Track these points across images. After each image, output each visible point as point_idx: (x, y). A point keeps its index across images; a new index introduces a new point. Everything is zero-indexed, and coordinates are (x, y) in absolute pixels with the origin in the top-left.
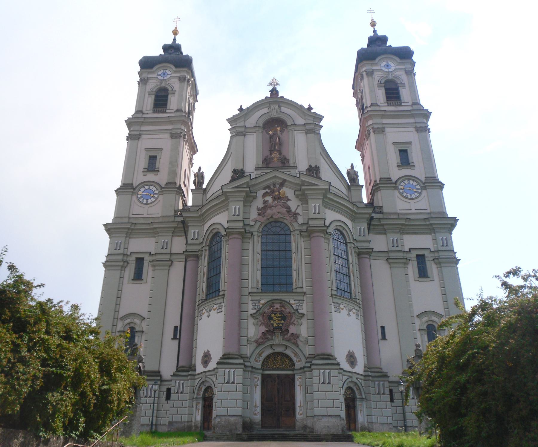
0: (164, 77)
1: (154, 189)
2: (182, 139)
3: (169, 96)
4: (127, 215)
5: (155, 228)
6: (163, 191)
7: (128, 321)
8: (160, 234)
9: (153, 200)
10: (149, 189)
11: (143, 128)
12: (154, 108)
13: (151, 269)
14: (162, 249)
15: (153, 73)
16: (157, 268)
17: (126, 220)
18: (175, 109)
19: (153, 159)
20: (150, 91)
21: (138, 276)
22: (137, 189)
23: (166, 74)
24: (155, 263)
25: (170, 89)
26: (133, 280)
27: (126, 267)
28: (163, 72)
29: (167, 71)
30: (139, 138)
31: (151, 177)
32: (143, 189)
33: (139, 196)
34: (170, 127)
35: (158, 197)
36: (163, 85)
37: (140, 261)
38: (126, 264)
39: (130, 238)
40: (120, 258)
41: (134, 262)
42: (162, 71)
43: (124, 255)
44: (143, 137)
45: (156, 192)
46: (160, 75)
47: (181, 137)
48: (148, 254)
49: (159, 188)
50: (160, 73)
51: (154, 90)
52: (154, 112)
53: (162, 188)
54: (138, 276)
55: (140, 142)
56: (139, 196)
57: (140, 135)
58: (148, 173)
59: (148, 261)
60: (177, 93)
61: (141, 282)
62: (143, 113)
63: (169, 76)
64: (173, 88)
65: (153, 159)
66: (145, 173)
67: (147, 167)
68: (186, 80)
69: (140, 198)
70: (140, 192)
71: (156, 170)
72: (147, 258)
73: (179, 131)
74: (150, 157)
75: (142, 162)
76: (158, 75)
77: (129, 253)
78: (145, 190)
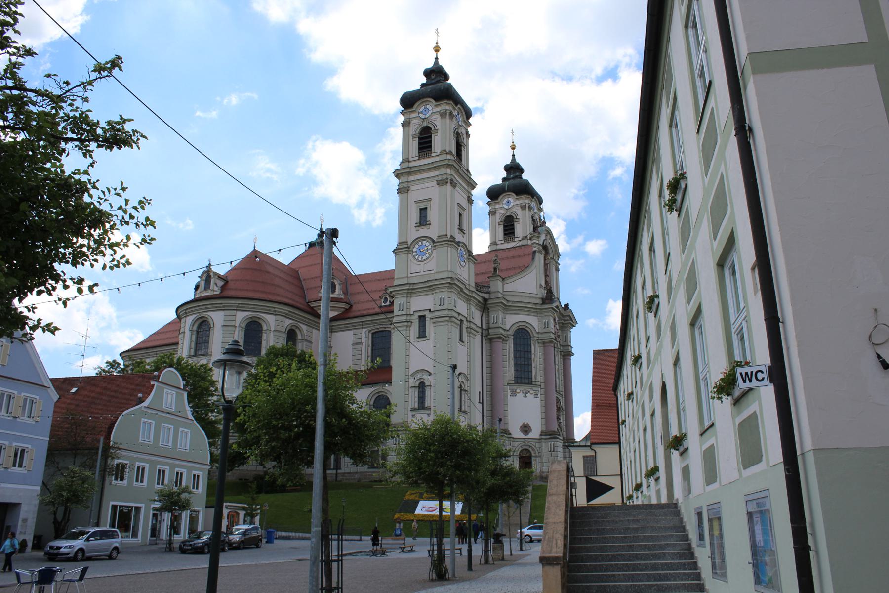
0: (425, 115)
1: (428, 244)
2: (449, 184)
3: (433, 136)
4: (406, 276)
5: (431, 286)
6: (435, 246)
7: (417, 377)
8: (437, 291)
9: (428, 256)
10: (422, 245)
11: (412, 178)
12: (419, 152)
13: (432, 325)
14: (440, 305)
15: (414, 111)
16: (437, 324)
19: (423, 211)
20: (414, 134)
21: (422, 334)
23: (427, 110)
24: (434, 320)
25: (433, 129)
26: (418, 338)
27: (410, 326)
29: (429, 107)
30: (408, 190)
31: (423, 232)
32: (417, 246)
33: (414, 254)
35: (432, 252)
36: (425, 124)
37: (422, 318)
38: (410, 323)
39: (411, 297)
40: (404, 318)
41: (418, 320)
42: (423, 108)
43: (407, 315)
44: (412, 188)
45: (430, 247)
46: (422, 112)
47: (447, 183)
48: (428, 312)
49: (432, 243)
50: (421, 110)
51: (418, 132)
52: (420, 159)
53: (434, 242)
54: (422, 334)
55: (409, 195)
56: (414, 254)
57: (409, 187)
58: (420, 227)
59: (429, 319)
60: (439, 132)
61: (425, 339)
62: (409, 162)
64: (435, 126)
65: (423, 211)
66: (418, 228)
67: (418, 222)
68: (448, 114)
69: (416, 255)
70: (415, 250)
71: (428, 223)
72: (428, 315)
73: (444, 177)
74: (421, 209)
75: (414, 217)
76: (419, 113)
77: (412, 313)
78: (419, 246)
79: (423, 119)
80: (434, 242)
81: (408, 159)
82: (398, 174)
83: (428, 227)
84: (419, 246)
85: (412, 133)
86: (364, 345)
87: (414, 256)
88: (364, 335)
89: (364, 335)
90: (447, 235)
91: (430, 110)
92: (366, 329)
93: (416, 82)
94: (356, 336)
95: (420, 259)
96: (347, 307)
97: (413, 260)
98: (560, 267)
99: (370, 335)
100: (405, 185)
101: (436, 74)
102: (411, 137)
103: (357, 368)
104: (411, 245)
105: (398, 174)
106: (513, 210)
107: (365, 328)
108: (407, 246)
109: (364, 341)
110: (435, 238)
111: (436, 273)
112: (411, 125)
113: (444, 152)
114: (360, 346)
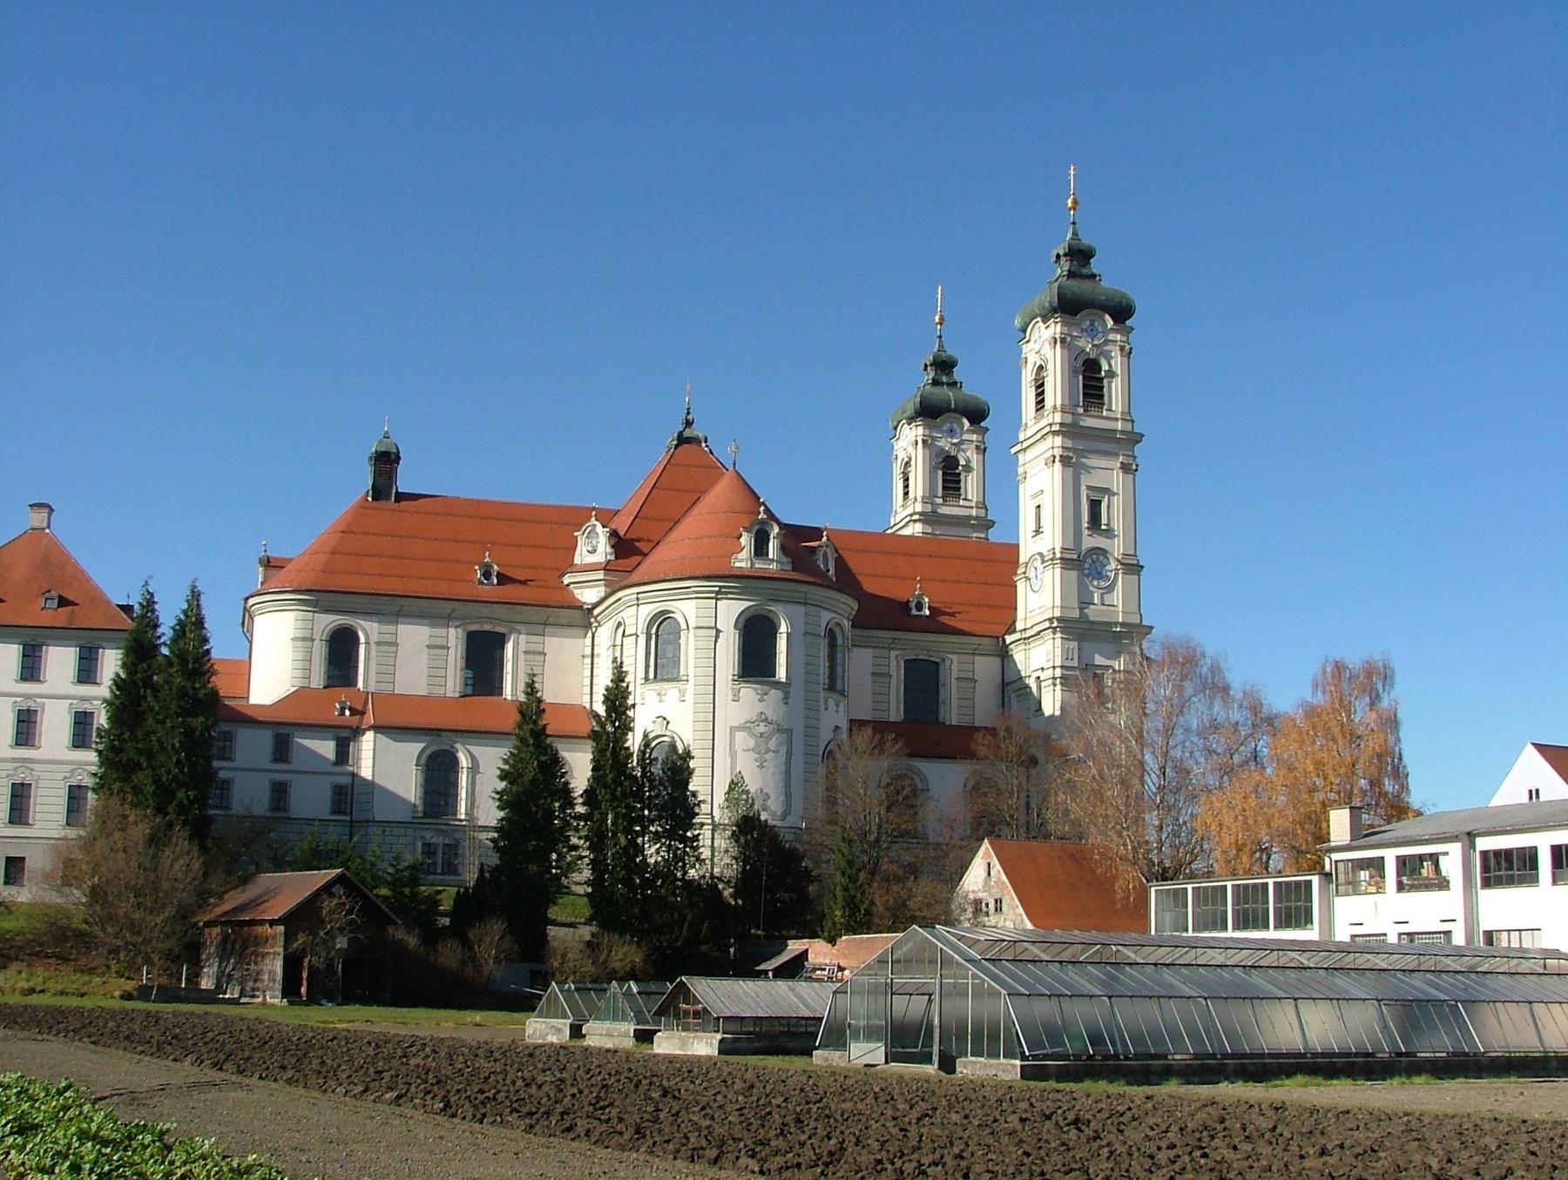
10: (1098, 559)
15: (1076, 325)
17: (1076, 614)
42: (1088, 323)
50: (1084, 327)
56: (1086, 572)
65: (1095, 506)
86: (894, 680)
88: (893, 663)
89: (893, 663)
92: (898, 653)
94: (880, 661)
99: (902, 663)
103: (882, 716)
107: (894, 649)
109: (893, 672)
114: (887, 680)
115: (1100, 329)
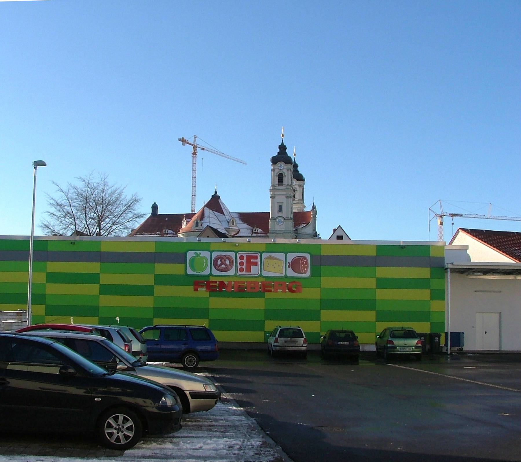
0: (281, 168)
1: (282, 219)
9: (282, 223)
15: (276, 166)
18: (286, 184)
19: (280, 208)
22: (276, 220)
25: (284, 175)
28: (281, 165)
29: (282, 165)
31: (280, 214)
32: (278, 219)
34: (285, 193)
42: (280, 165)
44: (277, 197)
46: (279, 167)
50: (279, 166)
51: (278, 174)
53: (284, 218)
58: (279, 213)
63: (283, 167)
64: (285, 173)
65: (280, 208)
73: (288, 195)
74: (279, 206)
75: (277, 209)
76: (278, 167)
79: (281, 170)
80: (284, 218)
81: (274, 185)
82: (271, 190)
83: (282, 213)
84: (279, 220)
85: (275, 174)
87: (277, 223)
90: (289, 217)
91: (282, 166)
93: (275, 152)
95: (279, 224)
96: (238, 230)
97: (277, 225)
98: (317, 219)
100: (274, 196)
101: (282, 148)
102: (275, 176)
104: (276, 218)
105: (271, 190)
106: (296, 186)
108: (274, 219)
110: (285, 218)
111: (285, 230)
112: (275, 171)
113: (288, 185)
115: (283, 166)
